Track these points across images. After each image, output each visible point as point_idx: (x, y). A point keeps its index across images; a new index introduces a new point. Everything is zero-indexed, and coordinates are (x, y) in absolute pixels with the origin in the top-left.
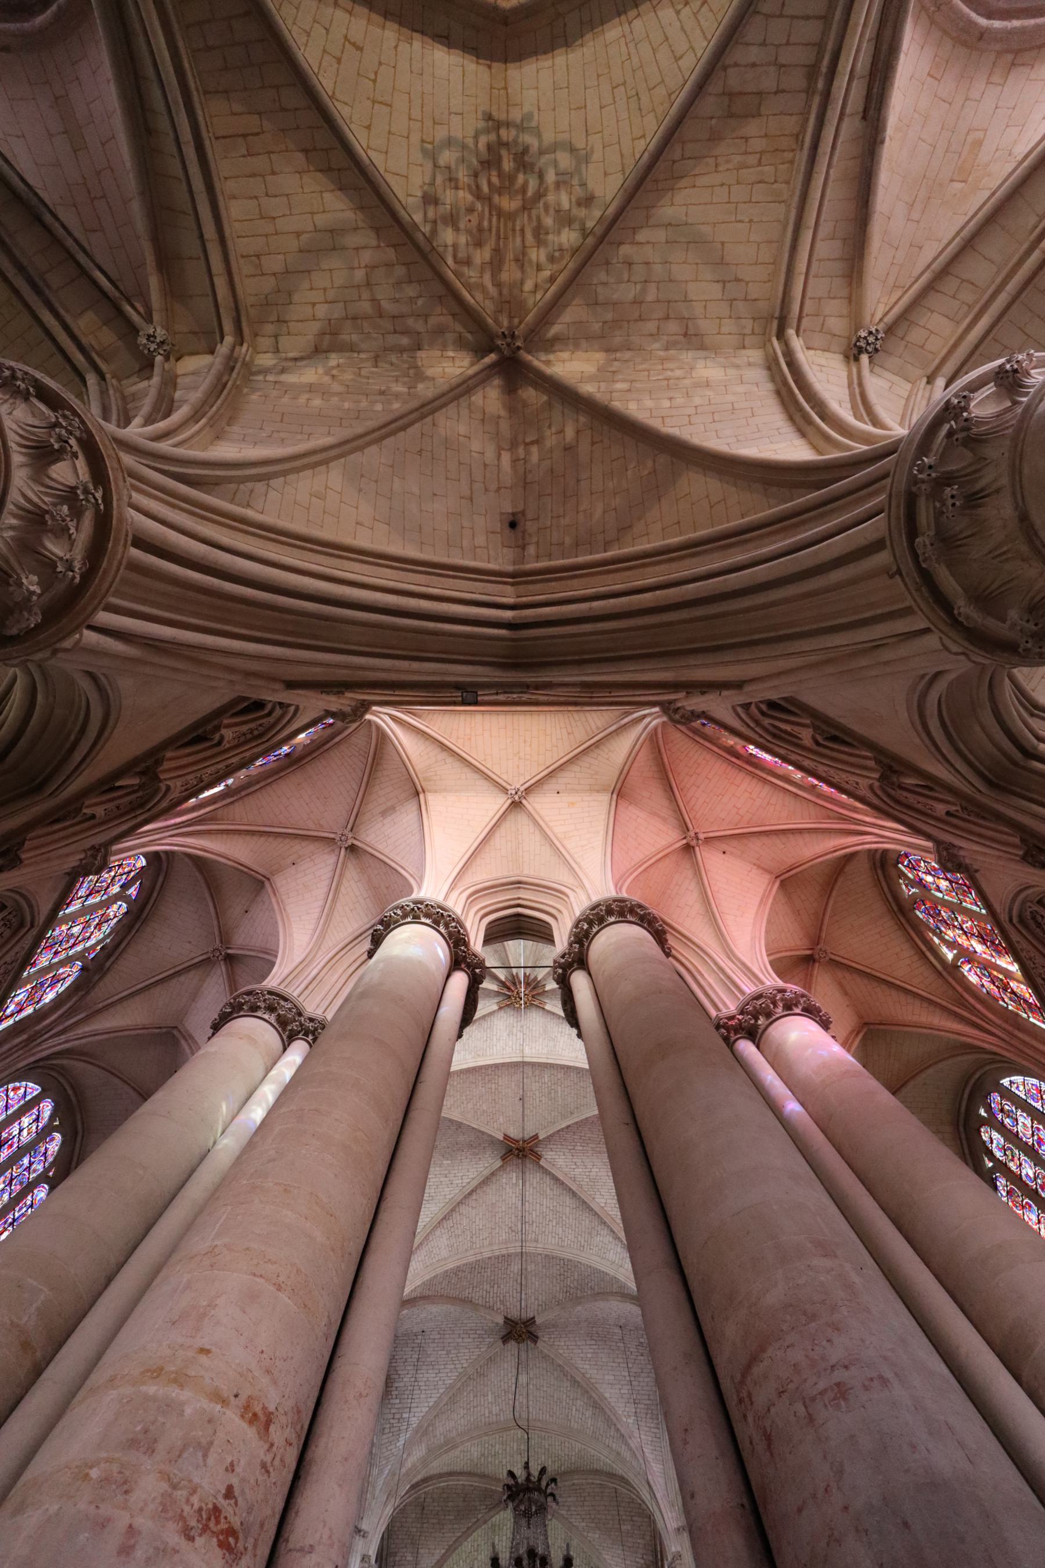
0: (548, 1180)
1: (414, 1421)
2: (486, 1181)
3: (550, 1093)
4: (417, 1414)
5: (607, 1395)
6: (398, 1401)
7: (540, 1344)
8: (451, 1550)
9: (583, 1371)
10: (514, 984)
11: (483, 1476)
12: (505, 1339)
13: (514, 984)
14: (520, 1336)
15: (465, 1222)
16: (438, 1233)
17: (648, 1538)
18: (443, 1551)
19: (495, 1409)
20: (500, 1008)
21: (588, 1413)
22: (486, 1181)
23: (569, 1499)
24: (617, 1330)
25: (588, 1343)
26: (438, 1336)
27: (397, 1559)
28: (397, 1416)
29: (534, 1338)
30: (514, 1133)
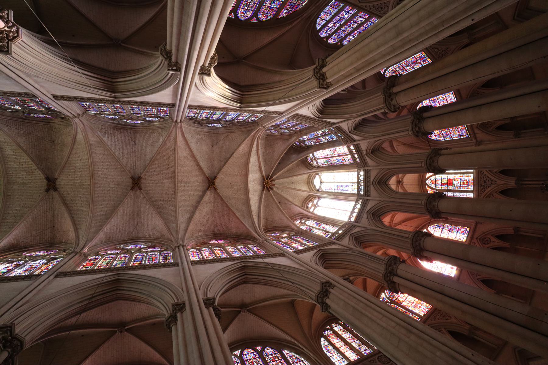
0: (200, 193)
1: (105, 139)
2: (201, 169)
3: (234, 193)
4: (108, 140)
5: (112, 220)
6: (111, 132)
7: (131, 192)
8: (25, 151)
9: (120, 210)
10: (271, 181)
11: (64, 167)
12: (132, 178)
13: (271, 181)
14: (136, 183)
15: (188, 162)
16: (188, 152)
17: (31, 243)
18: (24, 148)
19: (100, 173)
20: (263, 177)
21: (102, 212)
22: (201, 169)
23: (45, 206)
24: (136, 223)
25: (130, 211)
26: (133, 150)
27: (21, 127)
28: (106, 131)
29: (132, 189)
30: (217, 180)
